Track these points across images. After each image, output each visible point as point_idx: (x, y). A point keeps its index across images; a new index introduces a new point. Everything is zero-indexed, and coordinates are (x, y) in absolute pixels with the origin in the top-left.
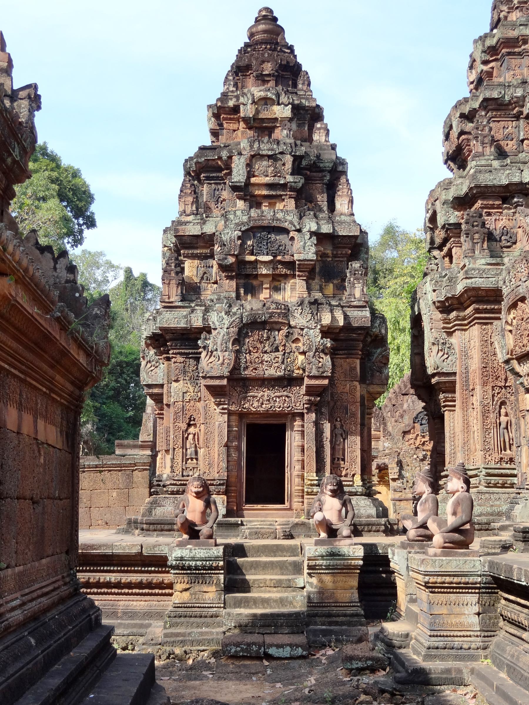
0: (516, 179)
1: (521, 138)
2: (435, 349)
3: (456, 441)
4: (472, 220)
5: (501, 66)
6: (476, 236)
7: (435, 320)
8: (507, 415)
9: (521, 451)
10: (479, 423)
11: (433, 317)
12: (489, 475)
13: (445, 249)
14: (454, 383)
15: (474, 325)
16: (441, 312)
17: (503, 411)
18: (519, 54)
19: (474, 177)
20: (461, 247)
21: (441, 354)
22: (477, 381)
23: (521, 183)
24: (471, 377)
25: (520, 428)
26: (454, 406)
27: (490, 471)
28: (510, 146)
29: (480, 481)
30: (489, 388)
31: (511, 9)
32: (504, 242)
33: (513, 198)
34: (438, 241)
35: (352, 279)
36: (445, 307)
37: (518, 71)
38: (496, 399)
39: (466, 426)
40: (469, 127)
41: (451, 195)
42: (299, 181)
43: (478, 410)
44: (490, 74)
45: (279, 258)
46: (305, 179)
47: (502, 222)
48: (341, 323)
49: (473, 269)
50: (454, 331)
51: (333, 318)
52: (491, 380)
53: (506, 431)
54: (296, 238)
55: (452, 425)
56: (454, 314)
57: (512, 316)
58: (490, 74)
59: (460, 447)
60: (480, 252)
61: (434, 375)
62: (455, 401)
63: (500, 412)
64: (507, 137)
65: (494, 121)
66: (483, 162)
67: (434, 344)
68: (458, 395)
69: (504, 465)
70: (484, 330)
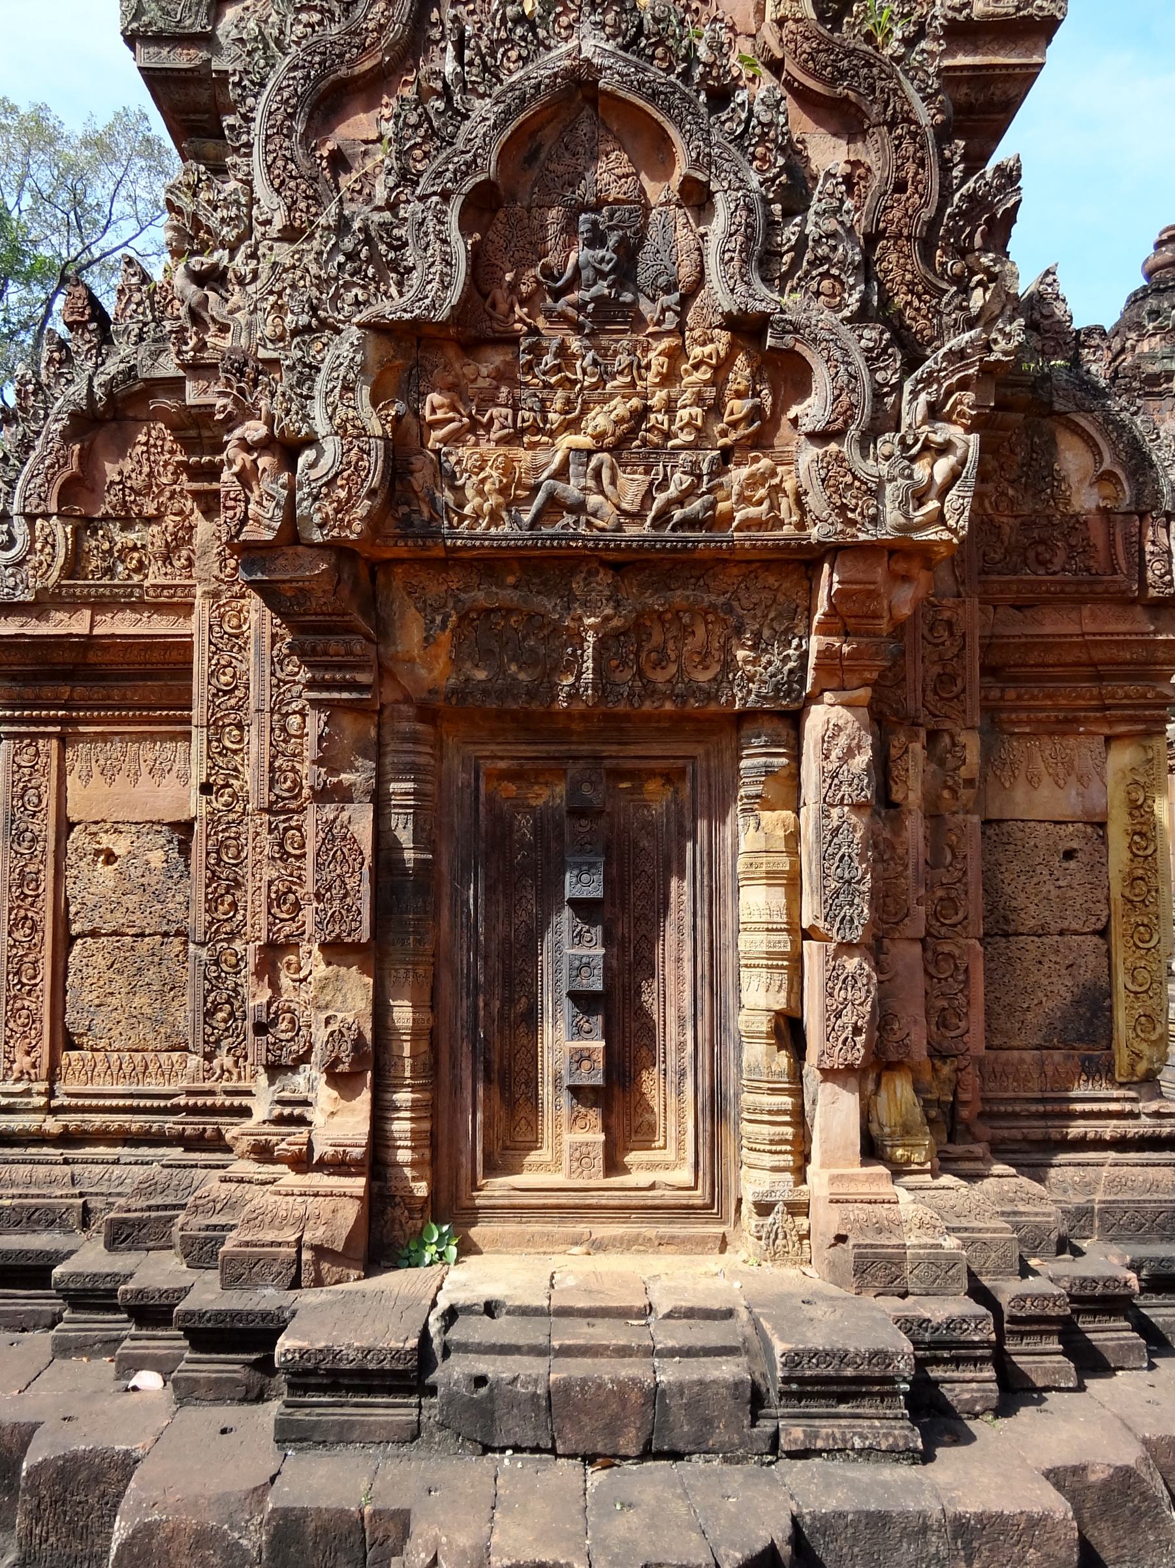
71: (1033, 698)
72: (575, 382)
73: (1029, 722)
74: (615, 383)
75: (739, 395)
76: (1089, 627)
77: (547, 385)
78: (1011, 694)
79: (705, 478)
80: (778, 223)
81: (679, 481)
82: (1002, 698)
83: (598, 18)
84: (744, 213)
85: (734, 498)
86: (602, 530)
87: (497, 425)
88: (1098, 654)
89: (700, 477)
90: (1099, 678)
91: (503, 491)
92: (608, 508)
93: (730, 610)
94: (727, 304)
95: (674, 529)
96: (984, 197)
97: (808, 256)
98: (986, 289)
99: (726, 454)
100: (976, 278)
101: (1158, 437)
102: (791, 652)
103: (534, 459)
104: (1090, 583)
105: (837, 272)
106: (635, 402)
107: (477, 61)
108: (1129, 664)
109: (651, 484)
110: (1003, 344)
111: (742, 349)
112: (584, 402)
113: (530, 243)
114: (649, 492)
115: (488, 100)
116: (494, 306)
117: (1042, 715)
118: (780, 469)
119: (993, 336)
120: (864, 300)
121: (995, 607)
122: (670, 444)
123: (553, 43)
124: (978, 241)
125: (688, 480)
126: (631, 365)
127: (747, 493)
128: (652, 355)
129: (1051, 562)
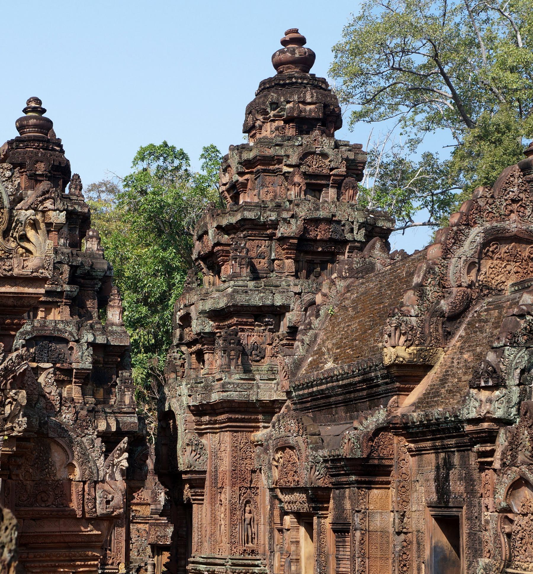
0: (269, 302)
1: (272, 258)
2: (189, 449)
3: (204, 532)
4: (229, 338)
5: (256, 179)
6: (233, 353)
7: (189, 422)
8: (250, 513)
9: (274, 556)
10: (227, 519)
11: (187, 419)
12: (234, 565)
13: (194, 348)
14: (204, 480)
15: (226, 431)
16: (195, 415)
17: (247, 508)
18: (273, 172)
19: (231, 296)
20: (213, 353)
21: (194, 454)
22: (227, 482)
23: (273, 305)
24: (220, 476)
25: (274, 537)
26: (203, 500)
27: (235, 561)
28: (262, 264)
29: (227, 570)
30: (237, 488)
31: (266, 120)
32: (254, 356)
33: (265, 317)
34: (187, 338)
35: (123, 387)
36: (198, 411)
37: (271, 189)
38: (242, 498)
39: (214, 520)
40: (225, 238)
41: (208, 305)
42: (75, 288)
43: (227, 507)
44: (244, 185)
45: (58, 365)
46: (81, 286)
47: (253, 338)
48: (114, 429)
49: (229, 383)
50: (206, 433)
51: (108, 424)
52: (238, 481)
53: (249, 526)
54: (75, 348)
55: (200, 516)
56: (207, 418)
57: (279, 455)
58: (244, 185)
59: (207, 537)
60: (235, 368)
61: (186, 473)
62: (203, 495)
63: (245, 509)
64: (261, 256)
65: (250, 240)
66: (241, 283)
67: (188, 445)
68: (207, 490)
69: (247, 556)
70: (235, 437)
71: (41, 557)
73: (40, 567)
76: (63, 529)
78: (31, 555)
82: (28, 557)
88: (67, 539)
90: (70, 548)
96: (11, 369)
98: (12, 404)
100: (9, 400)
101: (94, 446)
104: (62, 511)
108: (82, 542)
110: (18, 429)
117: (45, 564)
119: (14, 425)
121: (24, 520)
124: (8, 386)
129: (47, 500)
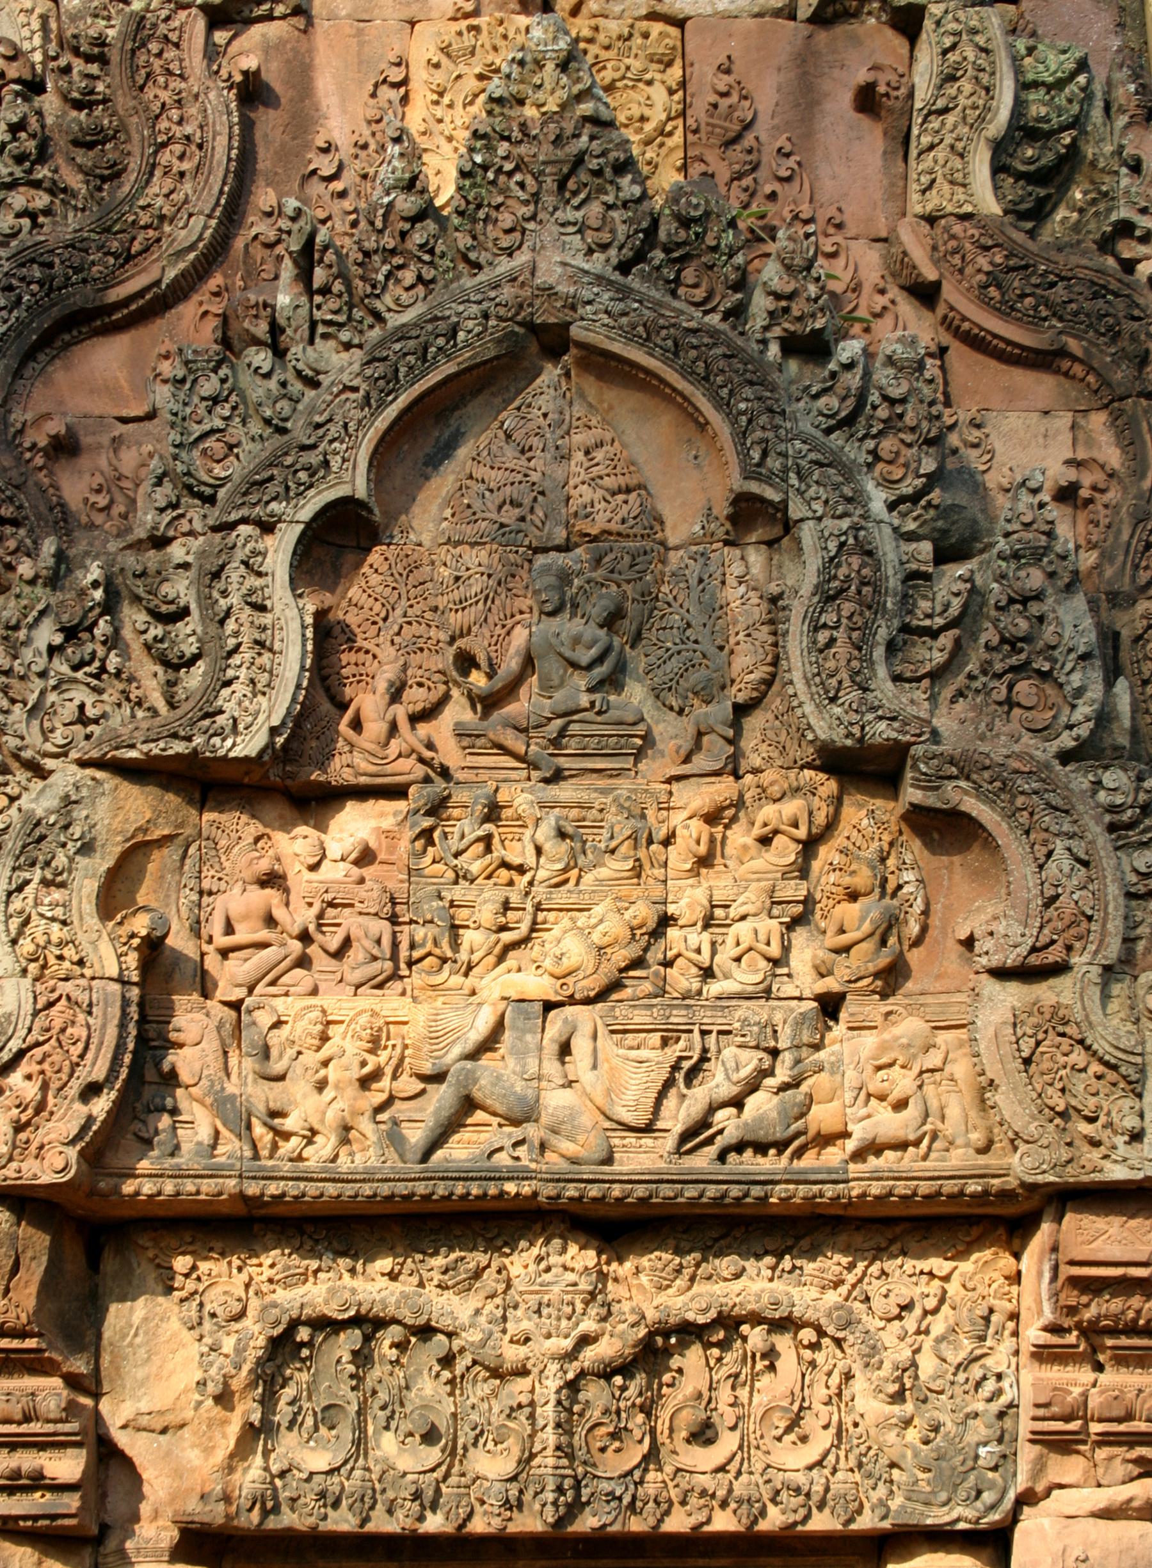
72: (521, 870)
74: (603, 872)
75: (853, 896)
77: (460, 876)
79: (787, 1058)
80: (927, 577)
81: (732, 1064)
83: (570, 215)
84: (855, 561)
85: (848, 1096)
86: (574, 1161)
87: (356, 954)
89: (775, 1053)
91: (365, 1083)
92: (588, 1118)
93: (848, 1324)
94: (826, 725)
95: (722, 1157)
97: (989, 635)
99: (830, 1006)
102: (980, 1406)
103: (435, 1017)
105: (1046, 667)
106: (643, 912)
107: (337, 287)
109: (675, 1068)
111: (860, 806)
112: (538, 908)
113: (435, 609)
114: (669, 1083)
115: (357, 354)
116: (357, 725)
118: (943, 1037)
120: (1104, 718)
122: (715, 988)
123: (484, 257)
125: (751, 1061)
126: (634, 837)
127: (874, 1086)
128: (677, 819)
